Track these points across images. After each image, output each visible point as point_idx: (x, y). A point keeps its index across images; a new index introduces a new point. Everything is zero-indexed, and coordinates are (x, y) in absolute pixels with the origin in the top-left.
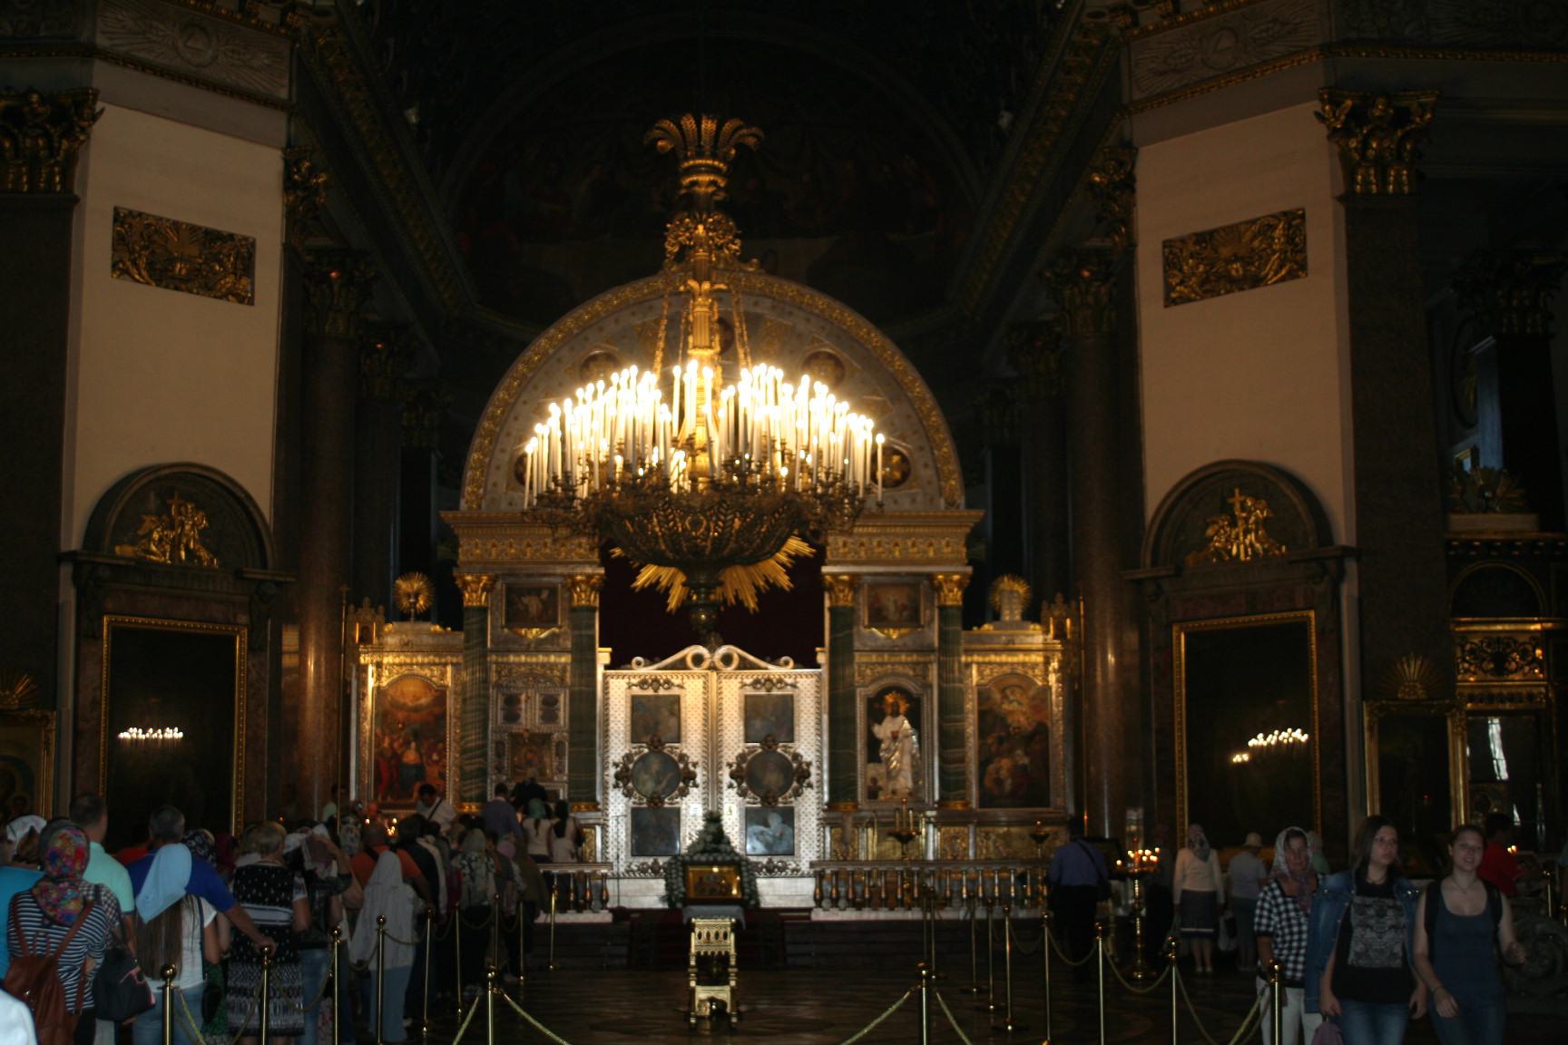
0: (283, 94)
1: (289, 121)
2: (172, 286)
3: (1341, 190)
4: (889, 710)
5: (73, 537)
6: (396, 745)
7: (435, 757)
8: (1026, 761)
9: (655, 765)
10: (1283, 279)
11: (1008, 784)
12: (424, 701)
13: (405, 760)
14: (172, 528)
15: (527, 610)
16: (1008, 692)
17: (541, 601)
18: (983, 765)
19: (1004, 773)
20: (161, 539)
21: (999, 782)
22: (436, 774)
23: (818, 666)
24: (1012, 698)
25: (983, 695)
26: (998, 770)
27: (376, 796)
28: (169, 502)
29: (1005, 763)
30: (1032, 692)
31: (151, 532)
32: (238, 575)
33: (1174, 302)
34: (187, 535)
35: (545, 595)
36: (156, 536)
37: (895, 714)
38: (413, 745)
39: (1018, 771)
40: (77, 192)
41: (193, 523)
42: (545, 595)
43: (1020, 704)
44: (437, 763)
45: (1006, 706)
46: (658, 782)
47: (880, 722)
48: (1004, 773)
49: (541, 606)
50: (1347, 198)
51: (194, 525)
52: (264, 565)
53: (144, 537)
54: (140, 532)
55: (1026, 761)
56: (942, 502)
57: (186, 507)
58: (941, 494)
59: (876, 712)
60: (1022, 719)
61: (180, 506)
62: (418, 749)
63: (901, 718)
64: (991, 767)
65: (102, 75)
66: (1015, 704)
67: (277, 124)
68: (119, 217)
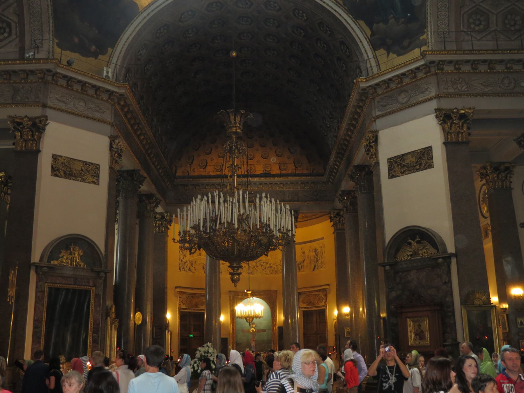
0: (109, 120)
1: (111, 128)
2: (72, 179)
3: (443, 141)
5: (36, 257)
10: (426, 169)
14: (71, 254)
20: (67, 258)
28: (70, 246)
31: (64, 256)
32: (92, 270)
34: (76, 257)
36: (65, 257)
40: (41, 149)
41: (78, 253)
50: (446, 144)
51: (79, 254)
52: (101, 267)
53: (61, 257)
54: (60, 256)
57: (76, 248)
61: (74, 248)
65: (49, 112)
67: (108, 129)
68: (55, 157)
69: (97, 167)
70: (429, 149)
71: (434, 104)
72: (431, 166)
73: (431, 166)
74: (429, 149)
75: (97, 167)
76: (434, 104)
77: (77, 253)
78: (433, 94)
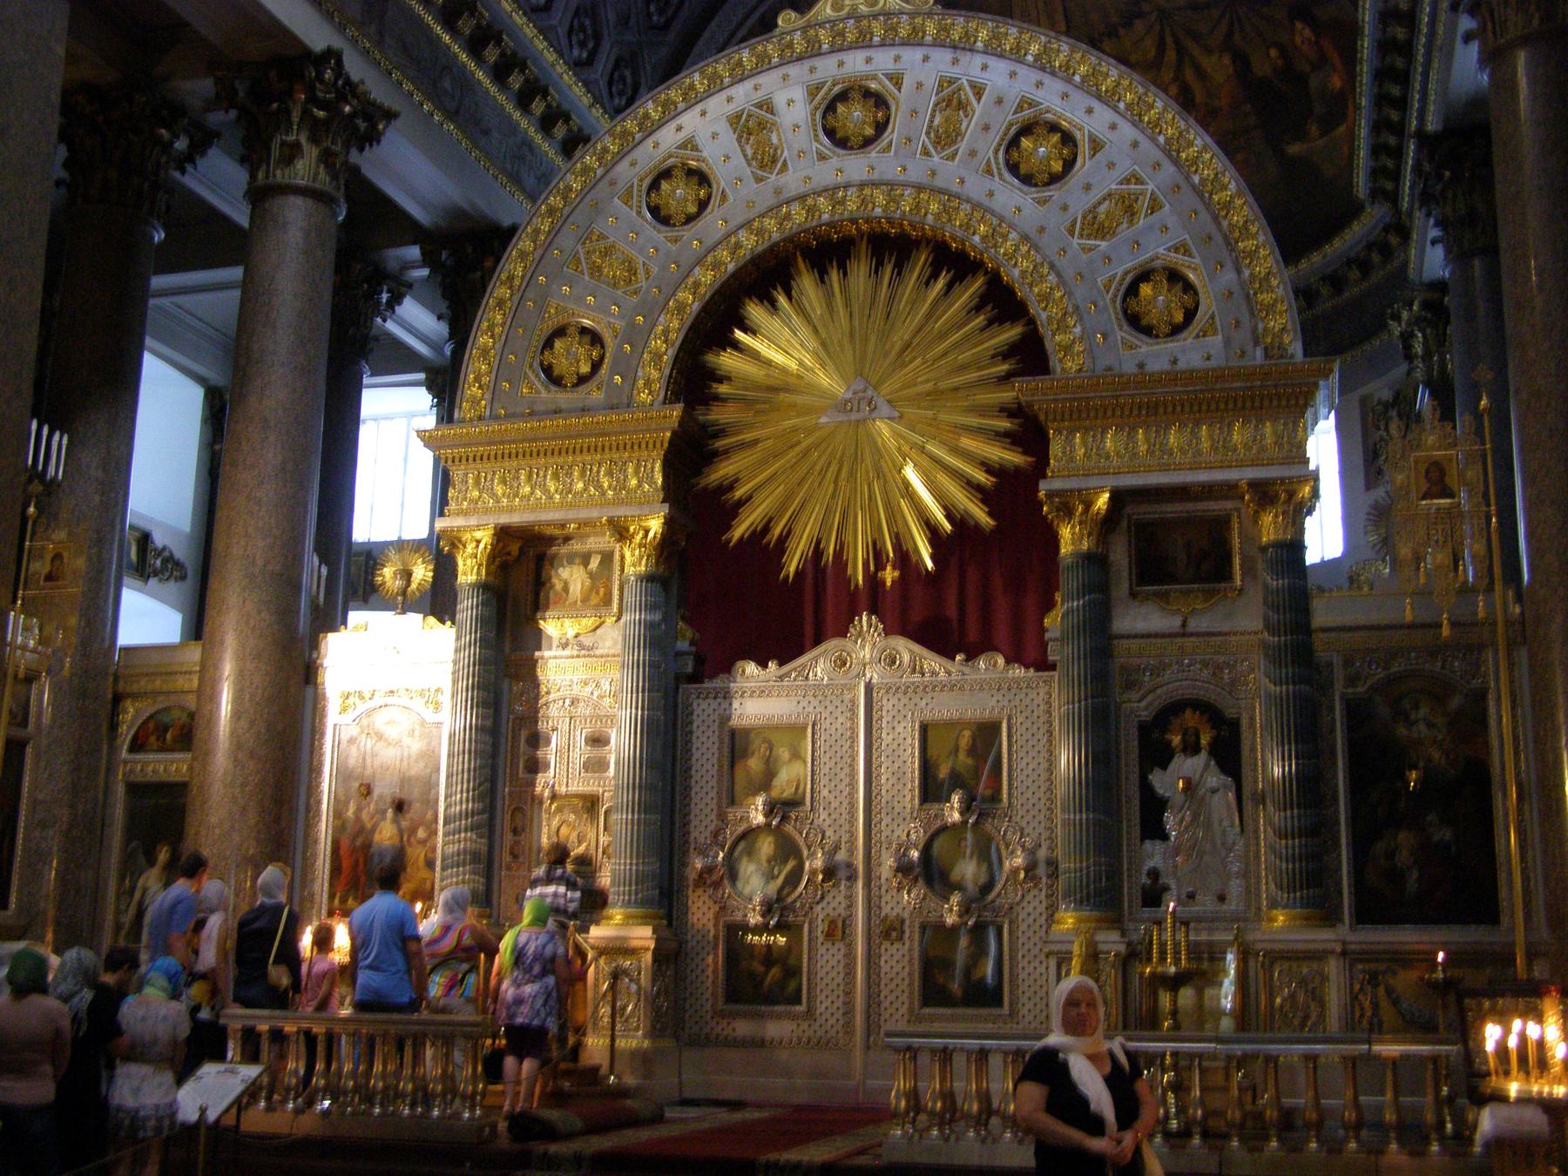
4: (1176, 740)
6: (365, 816)
7: (421, 834)
8: (1446, 834)
9: (766, 846)
13: (377, 837)
15: (566, 589)
16: (1406, 704)
17: (591, 575)
19: (1404, 857)
22: (421, 862)
23: (1053, 667)
24: (1413, 717)
25: (1357, 712)
26: (1390, 855)
27: (332, 897)
29: (1405, 839)
30: (1455, 702)
35: (594, 563)
37: (1192, 748)
38: (390, 813)
42: (594, 563)
43: (1430, 725)
44: (423, 842)
45: (1402, 731)
46: (770, 877)
47: (1164, 765)
48: (1404, 857)
49: (588, 583)
55: (1446, 834)
56: (1259, 353)
58: (1256, 343)
59: (1156, 755)
60: (1436, 755)
62: (395, 821)
63: (1203, 756)
64: (1380, 847)
66: (1422, 727)
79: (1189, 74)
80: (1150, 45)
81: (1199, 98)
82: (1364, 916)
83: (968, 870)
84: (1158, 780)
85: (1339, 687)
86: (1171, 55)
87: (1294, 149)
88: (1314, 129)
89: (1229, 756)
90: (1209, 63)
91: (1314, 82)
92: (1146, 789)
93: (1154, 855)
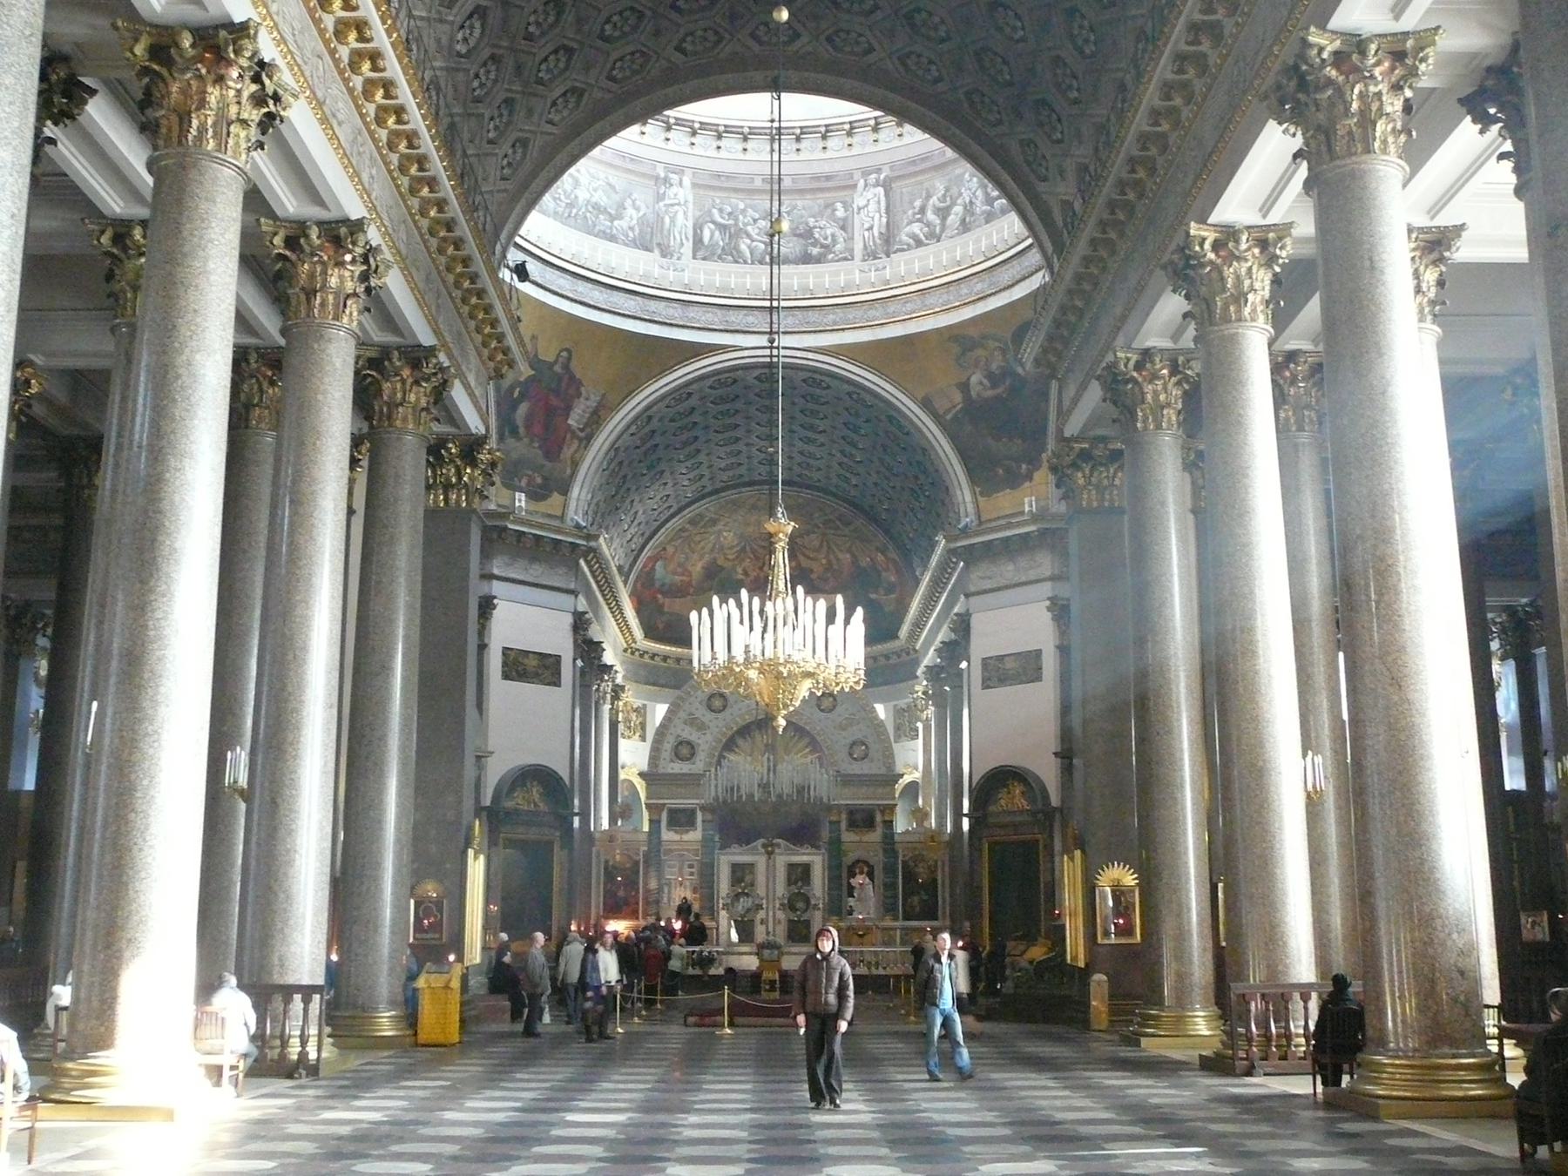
8: (925, 897)
11: (918, 909)
12: (628, 865)
18: (904, 900)
21: (913, 907)
29: (916, 899)
33: (988, 687)
37: (862, 873)
39: (922, 901)
40: (486, 641)
41: (536, 792)
69: (558, 659)
70: (1038, 653)
71: (1046, 589)
72: (1038, 678)
73: (1038, 678)
74: (1038, 653)
75: (558, 659)
76: (1046, 589)
77: (535, 790)
78: (1048, 573)
79: (832, 557)
80: (816, 543)
81: (835, 567)
82: (906, 918)
83: (800, 905)
84: (852, 881)
85: (900, 858)
86: (825, 548)
87: (873, 596)
88: (882, 592)
89: (871, 875)
90: (841, 556)
91: (884, 574)
92: (849, 884)
93: (851, 902)
